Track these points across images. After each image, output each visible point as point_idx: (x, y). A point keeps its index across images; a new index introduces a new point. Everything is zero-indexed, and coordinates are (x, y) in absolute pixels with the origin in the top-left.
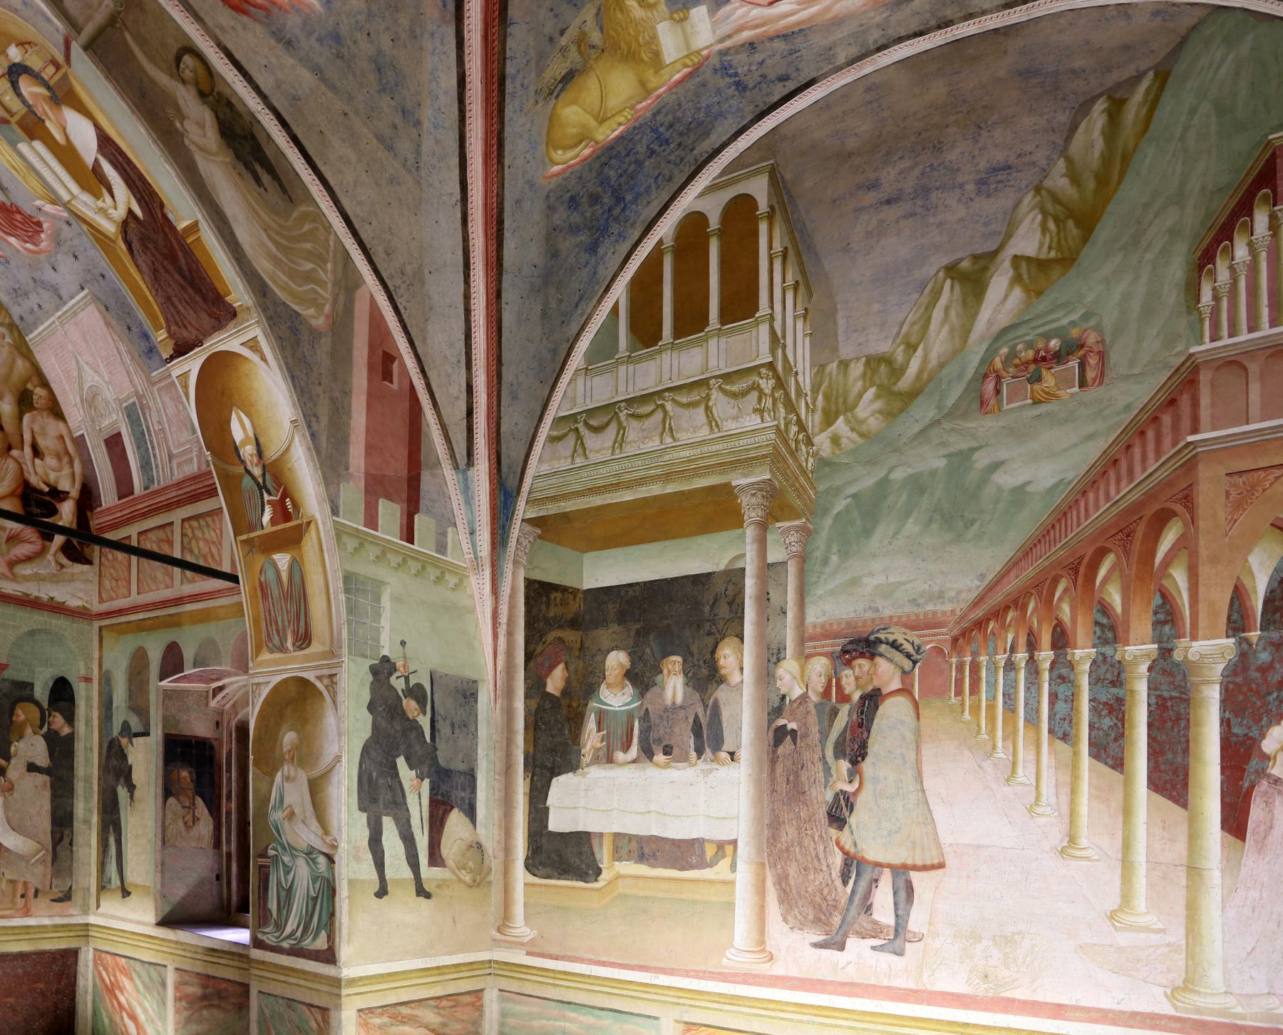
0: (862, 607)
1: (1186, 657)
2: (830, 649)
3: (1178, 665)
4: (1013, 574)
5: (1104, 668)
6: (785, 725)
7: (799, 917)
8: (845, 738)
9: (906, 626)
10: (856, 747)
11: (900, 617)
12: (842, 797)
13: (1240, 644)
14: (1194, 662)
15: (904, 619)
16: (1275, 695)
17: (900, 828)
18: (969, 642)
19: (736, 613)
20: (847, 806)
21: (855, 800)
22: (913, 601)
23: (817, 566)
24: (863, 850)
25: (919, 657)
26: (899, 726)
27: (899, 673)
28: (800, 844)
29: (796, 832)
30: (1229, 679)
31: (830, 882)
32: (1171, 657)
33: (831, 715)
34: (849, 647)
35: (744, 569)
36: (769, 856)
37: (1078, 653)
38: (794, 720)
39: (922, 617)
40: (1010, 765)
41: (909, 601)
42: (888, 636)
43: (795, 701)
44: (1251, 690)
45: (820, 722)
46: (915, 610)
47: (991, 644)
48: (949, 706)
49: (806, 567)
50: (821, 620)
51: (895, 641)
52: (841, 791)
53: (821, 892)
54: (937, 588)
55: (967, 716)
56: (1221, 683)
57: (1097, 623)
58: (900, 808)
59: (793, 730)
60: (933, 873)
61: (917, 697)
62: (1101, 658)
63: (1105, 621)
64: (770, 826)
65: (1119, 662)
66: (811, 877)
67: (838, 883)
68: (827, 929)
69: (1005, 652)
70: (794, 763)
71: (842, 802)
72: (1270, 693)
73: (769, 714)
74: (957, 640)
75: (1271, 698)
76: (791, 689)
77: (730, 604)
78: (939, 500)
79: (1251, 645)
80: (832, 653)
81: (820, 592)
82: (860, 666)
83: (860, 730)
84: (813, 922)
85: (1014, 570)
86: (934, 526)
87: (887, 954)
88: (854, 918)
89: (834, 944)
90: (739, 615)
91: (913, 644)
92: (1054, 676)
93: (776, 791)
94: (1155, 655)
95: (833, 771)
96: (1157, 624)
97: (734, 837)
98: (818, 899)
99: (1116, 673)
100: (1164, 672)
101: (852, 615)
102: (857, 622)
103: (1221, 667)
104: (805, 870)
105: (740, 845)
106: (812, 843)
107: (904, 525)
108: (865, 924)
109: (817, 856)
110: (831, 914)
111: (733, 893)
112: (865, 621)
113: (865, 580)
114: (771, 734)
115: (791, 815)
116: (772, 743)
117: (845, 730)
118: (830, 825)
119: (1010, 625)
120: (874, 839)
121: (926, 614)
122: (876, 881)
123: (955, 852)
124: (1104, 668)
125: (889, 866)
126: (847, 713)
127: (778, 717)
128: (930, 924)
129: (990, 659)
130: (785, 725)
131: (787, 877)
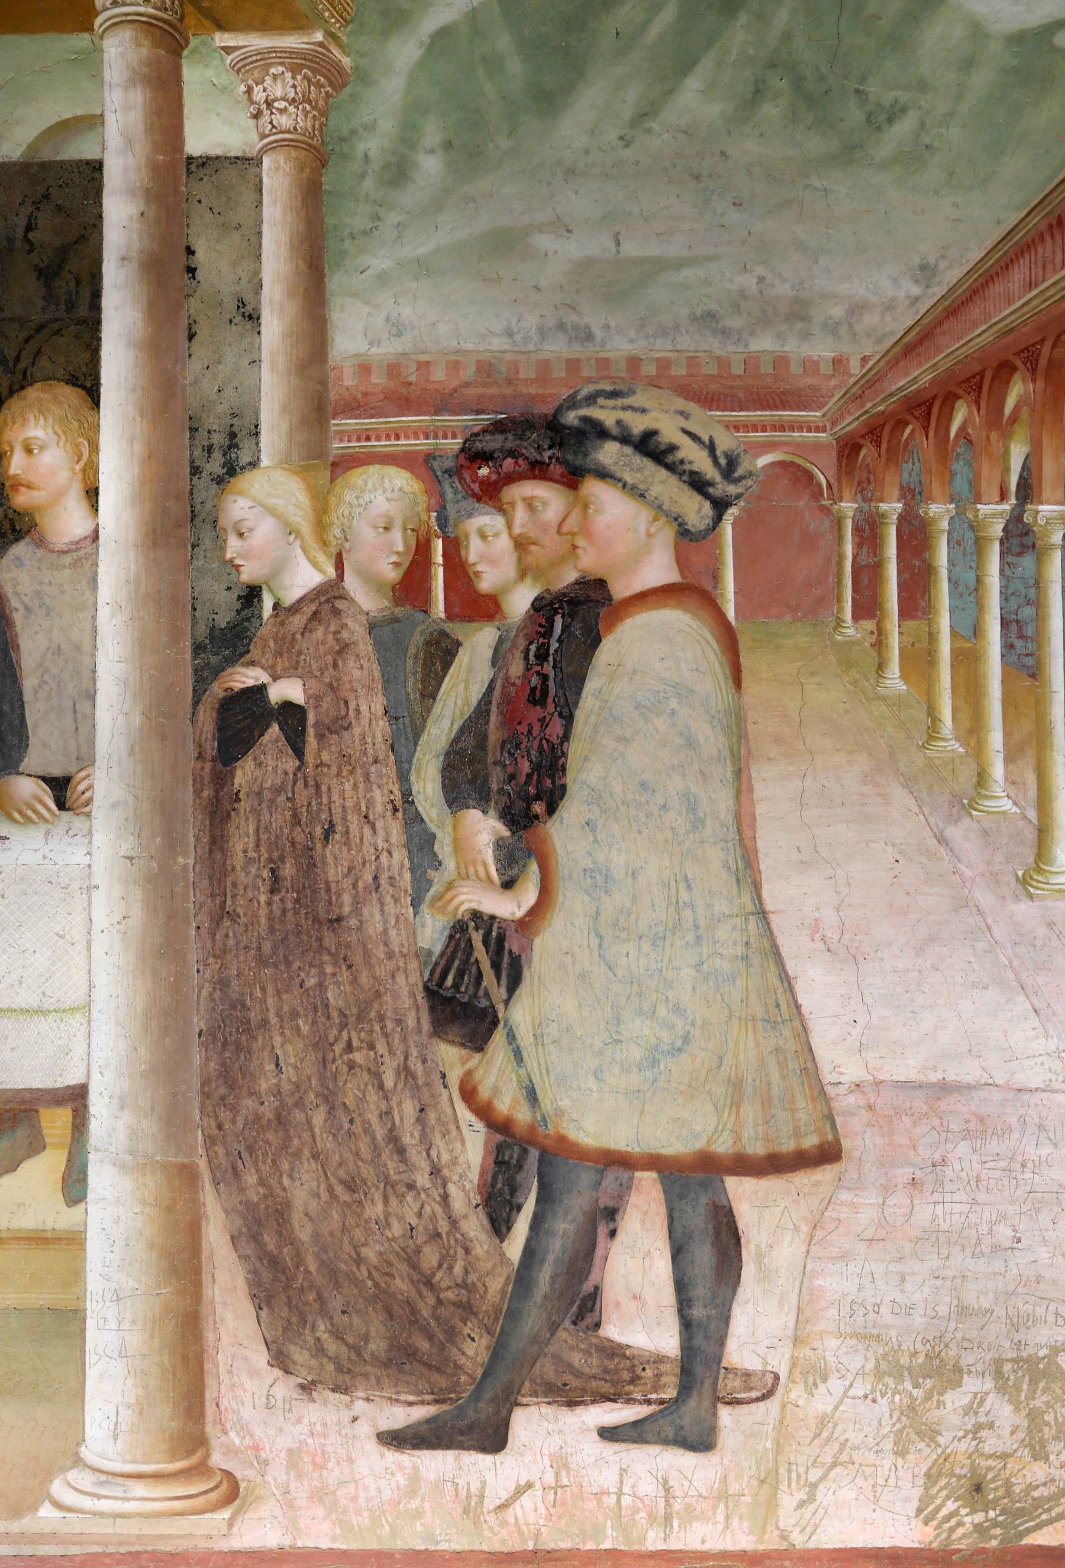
0: (531, 321)
2: (421, 444)
4: (1018, 274)
6: (260, 690)
7: (332, 1347)
8: (482, 741)
9: (685, 391)
10: (526, 767)
11: (664, 365)
12: (477, 938)
15: (679, 371)
17: (686, 1039)
18: (894, 456)
19: (71, 306)
20: (496, 966)
21: (528, 947)
22: (709, 318)
23: (368, 184)
24: (560, 1113)
25: (732, 489)
26: (674, 704)
27: (666, 535)
28: (329, 1099)
29: (312, 1057)
31: (443, 1226)
33: (428, 662)
34: (492, 443)
35: (97, 167)
36: (210, 1142)
38: (293, 670)
39: (738, 369)
40: (1030, 835)
41: (694, 318)
42: (628, 417)
43: (295, 608)
45: (388, 682)
46: (714, 345)
47: (958, 466)
48: (836, 645)
49: (328, 181)
50: (388, 348)
51: (650, 435)
52: (476, 915)
53: (412, 1259)
54: (784, 290)
55: (894, 679)
58: (687, 973)
59: (288, 706)
60: (803, 1179)
61: (731, 613)
64: (210, 1036)
66: (375, 1210)
67: (475, 1226)
68: (441, 1381)
69: (1003, 497)
70: (296, 820)
71: (480, 953)
73: (198, 648)
74: (857, 448)
76: (278, 569)
77: (48, 274)
80: (429, 457)
81: (380, 261)
82: (530, 504)
83: (537, 712)
84: (387, 1364)
85: (1024, 262)
86: (771, 111)
87: (654, 1450)
88: (535, 1339)
89: (470, 1428)
90: (82, 312)
91: (711, 448)
93: (233, 916)
95: (444, 848)
97: (73, 1078)
98: (401, 1285)
101: (498, 344)
102: (515, 367)
104: (350, 1186)
105: (98, 1106)
106: (373, 1096)
107: (670, 92)
108: (576, 1359)
109: (393, 1138)
110: (452, 1334)
111: (76, 1276)
112: (544, 366)
113: (543, 241)
114: (207, 718)
115: (292, 1000)
116: (211, 748)
117: (482, 711)
118: (439, 1029)
119: (1014, 419)
120: (598, 1075)
121: (751, 362)
122: (611, 1214)
123: (870, 1108)
125: (655, 1162)
126: (490, 653)
127: (231, 661)
128: (797, 1341)
129: (960, 513)
130: (260, 690)
131: (281, 1213)
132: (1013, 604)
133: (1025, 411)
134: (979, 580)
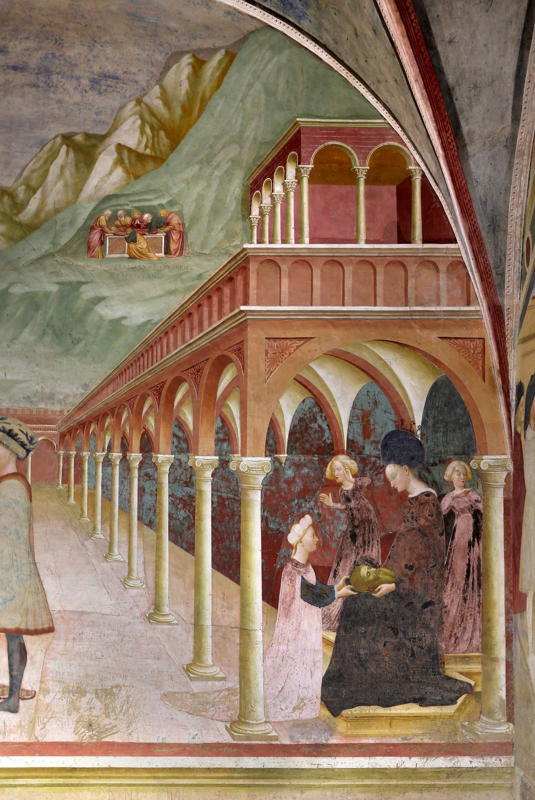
1: (238, 468)
3: (233, 474)
5: (180, 471)
13: (274, 462)
14: (244, 473)
16: (296, 501)
30: (267, 487)
32: (228, 467)
37: (161, 457)
44: (281, 496)
56: (262, 490)
57: (175, 435)
62: (177, 463)
63: (180, 434)
65: (191, 467)
72: (293, 500)
75: (293, 504)
78: (52, 318)
79: (281, 464)
92: (142, 474)
94: (216, 464)
96: (218, 441)
99: (188, 476)
100: (223, 478)
103: (262, 478)
124: (180, 471)
132: (105, 481)
133: (110, 428)
134: (96, 474)
